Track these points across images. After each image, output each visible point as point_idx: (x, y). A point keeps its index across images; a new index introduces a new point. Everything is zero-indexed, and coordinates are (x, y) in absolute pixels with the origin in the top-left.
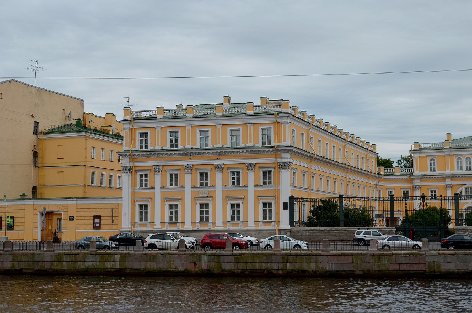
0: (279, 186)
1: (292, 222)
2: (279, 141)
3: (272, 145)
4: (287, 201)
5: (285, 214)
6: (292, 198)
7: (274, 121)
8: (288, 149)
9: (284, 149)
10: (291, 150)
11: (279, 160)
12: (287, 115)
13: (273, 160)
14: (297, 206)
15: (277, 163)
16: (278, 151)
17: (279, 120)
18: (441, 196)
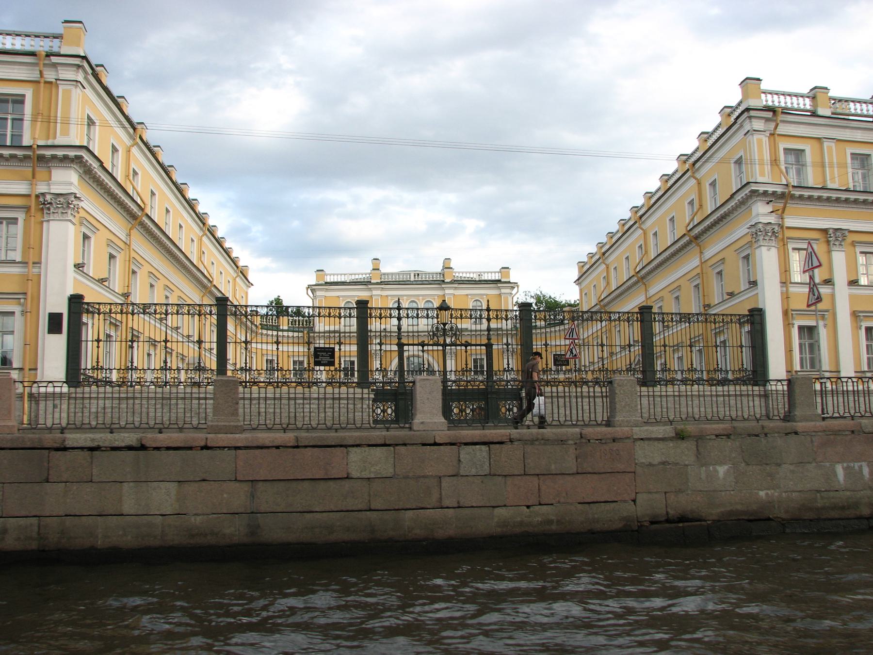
0: (38, 263)
1: (74, 372)
2: (49, 132)
3: (26, 141)
4: (63, 308)
5: (55, 348)
6: (76, 301)
7: (34, 75)
8: (72, 153)
9: (60, 153)
10: (77, 159)
11: (41, 188)
12: (77, 61)
13: (21, 188)
14: (92, 328)
15: (37, 196)
16: (41, 160)
17: (50, 75)
18: (488, 310)
